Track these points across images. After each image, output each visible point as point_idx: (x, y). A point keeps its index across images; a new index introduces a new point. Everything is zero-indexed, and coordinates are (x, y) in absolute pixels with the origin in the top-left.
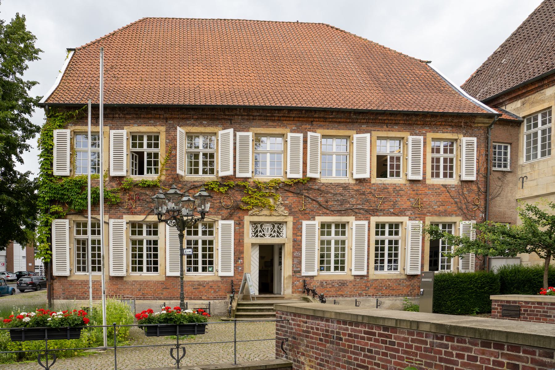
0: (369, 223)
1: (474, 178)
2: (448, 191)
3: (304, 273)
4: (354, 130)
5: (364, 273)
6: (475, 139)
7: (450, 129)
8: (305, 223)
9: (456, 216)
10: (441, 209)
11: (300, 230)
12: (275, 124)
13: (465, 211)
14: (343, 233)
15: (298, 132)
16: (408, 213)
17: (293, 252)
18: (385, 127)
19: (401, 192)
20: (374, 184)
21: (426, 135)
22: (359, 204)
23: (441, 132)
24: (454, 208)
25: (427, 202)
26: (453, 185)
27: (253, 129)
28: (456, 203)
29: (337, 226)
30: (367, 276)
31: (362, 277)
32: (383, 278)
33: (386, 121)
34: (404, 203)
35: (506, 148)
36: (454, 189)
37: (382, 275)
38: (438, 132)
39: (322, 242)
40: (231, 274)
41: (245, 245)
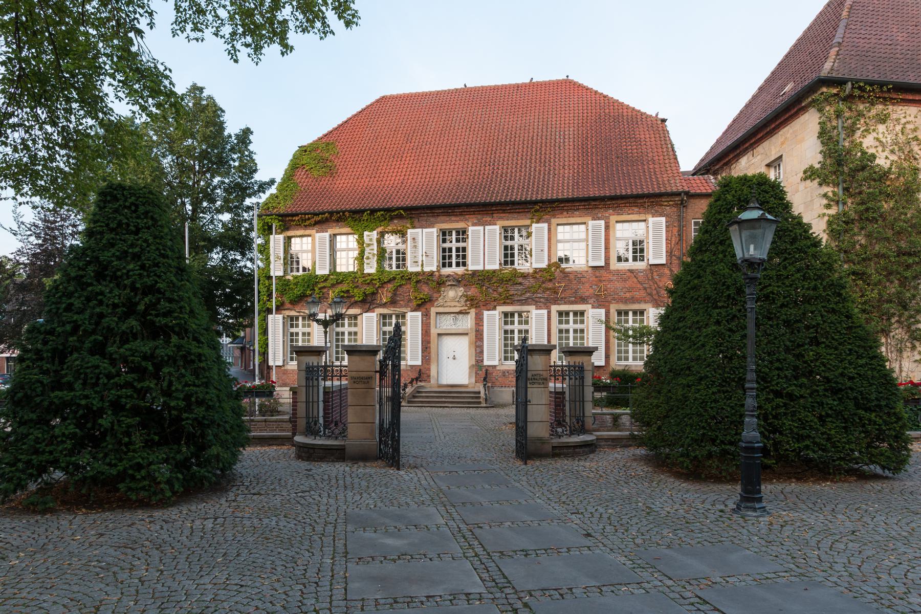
0: (549, 313)
1: (664, 262)
3: (486, 363)
6: (663, 219)
7: (636, 209)
8: (486, 313)
9: (646, 303)
10: (628, 295)
11: (482, 320)
13: (656, 297)
14: (582, 322)
15: (479, 225)
16: (591, 301)
24: (642, 294)
28: (645, 289)
29: (575, 314)
33: (565, 208)
34: (586, 290)
39: (561, 331)
40: (419, 363)
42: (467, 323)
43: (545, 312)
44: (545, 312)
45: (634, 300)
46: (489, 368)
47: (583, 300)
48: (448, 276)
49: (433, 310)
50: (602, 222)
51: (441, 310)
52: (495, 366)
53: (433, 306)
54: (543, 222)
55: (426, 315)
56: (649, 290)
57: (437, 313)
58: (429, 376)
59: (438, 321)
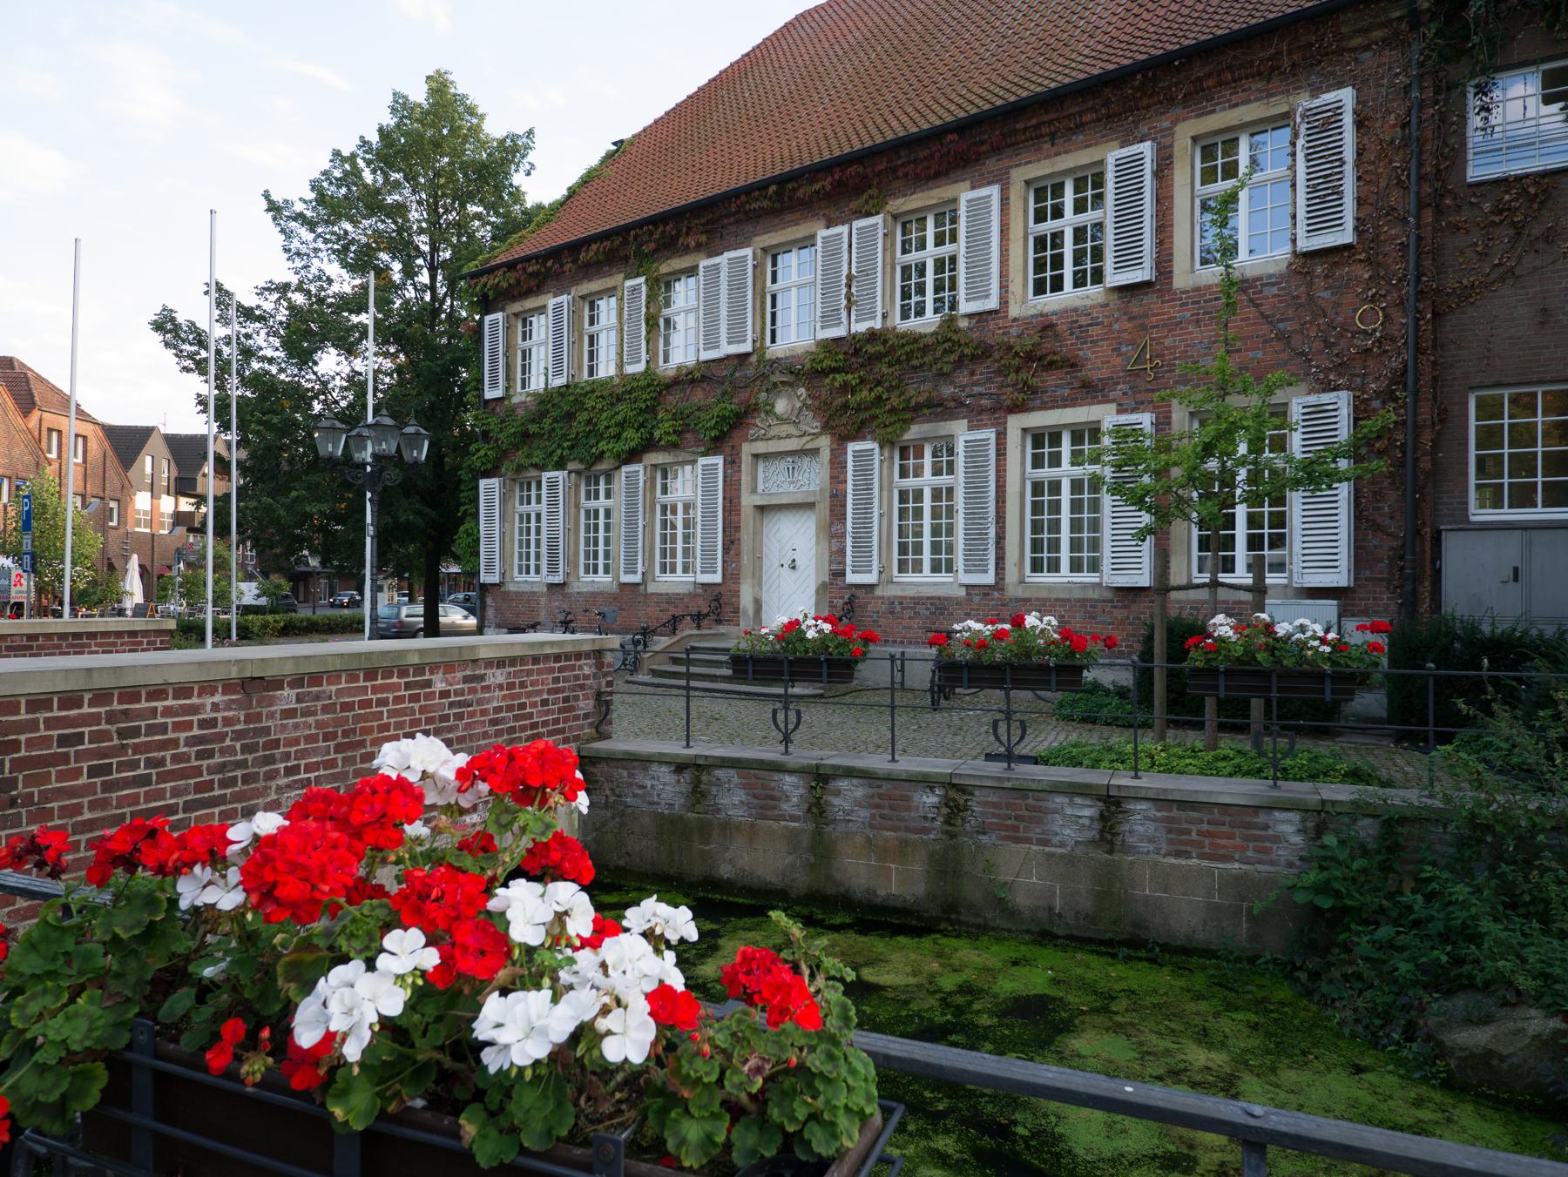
2: (1251, 300)
3: (851, 578)
4: (964, 180)
5: (989, 578)
12: (798, 215)
17: (831, 524)
18: (1047, 146)
19: (1095, 331)
20: (1015, 320)
21: (1172, 135)
22: (976, 384)
23: (1224, 109)
25: (1175, 347)
26: (1270, 276)
27: (757, 239)
28: (1284, 338)
30: (999, 585)
31: (985, 590)
32: (1044, 595)
36: (1274, 290)
37: (1051, 587)
38: (1214, 111)
40: (717, 578)
42: (812, 478)
43: (989, 434)
44: (989, 434)
46: (859, 593)
47: (1090, 391)
49: (747, 449)
51: (761, 447)
52: (870, 587)
53: (746, 440)
55: (732, 463)
56: (1296, 341)
58: (736, 610)
59: (761, 476)
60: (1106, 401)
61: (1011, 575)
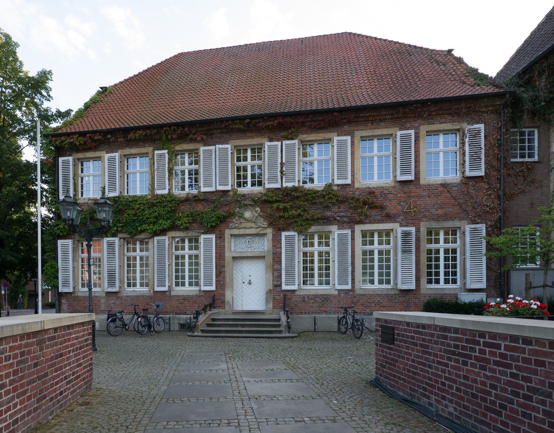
2: (448, 191)
3: (284, 287)
4: (334, 132)
5: (349, 287)
9: (460, 220)
10: (440, 212)
12: (254, 134)
17: (273, 265)
18: (370, 125)
19: (390, 196)
20: (357, 189)
21: (419, 129)
22: (341, 212)
23: (437, 124)
25: (421, 205)
26: (454, 183)
27: (232, 141)
30: (353, 289)
32: (371, 293)
33: (370, 118)
35: (531, 134)
36: (456, 188)
38: (434, 124)
40: (213, 288)
41: (226, 258)
43: (349, 232)
44: (349, 232)
45: (447, 217)
46: (287, 293)
47: (389, 218)
48: (244, 196)
49: (228, 232)
50: (412, 132)
51: (236, 232)
52: (294, 291)
54: (345, 135)
55: (220, 238)
57: (231, 235)
58: (223, 302)
59: (233, 244)
60: (395, 222)
61: (357, 287)
